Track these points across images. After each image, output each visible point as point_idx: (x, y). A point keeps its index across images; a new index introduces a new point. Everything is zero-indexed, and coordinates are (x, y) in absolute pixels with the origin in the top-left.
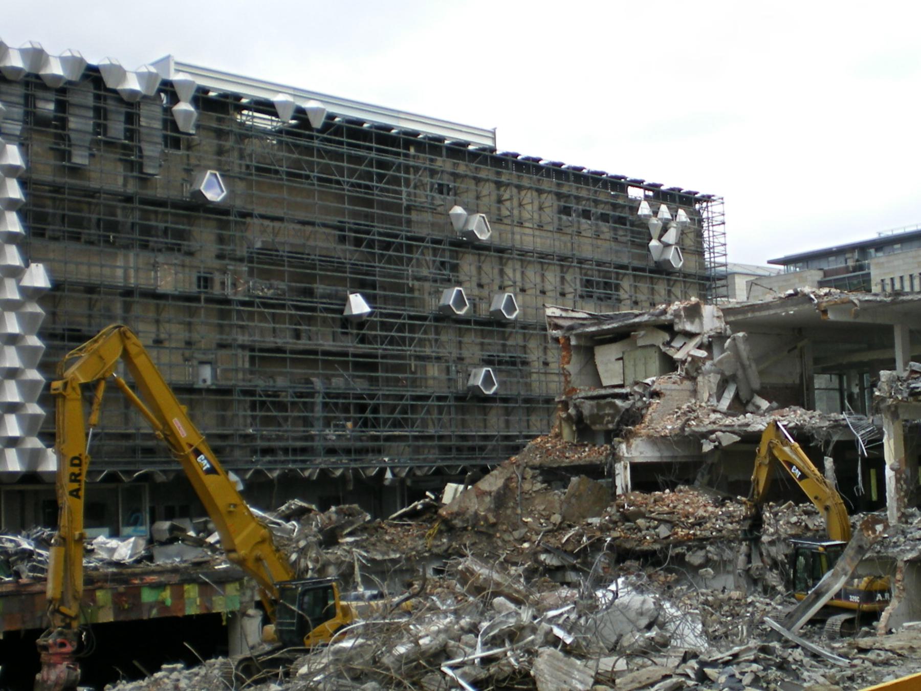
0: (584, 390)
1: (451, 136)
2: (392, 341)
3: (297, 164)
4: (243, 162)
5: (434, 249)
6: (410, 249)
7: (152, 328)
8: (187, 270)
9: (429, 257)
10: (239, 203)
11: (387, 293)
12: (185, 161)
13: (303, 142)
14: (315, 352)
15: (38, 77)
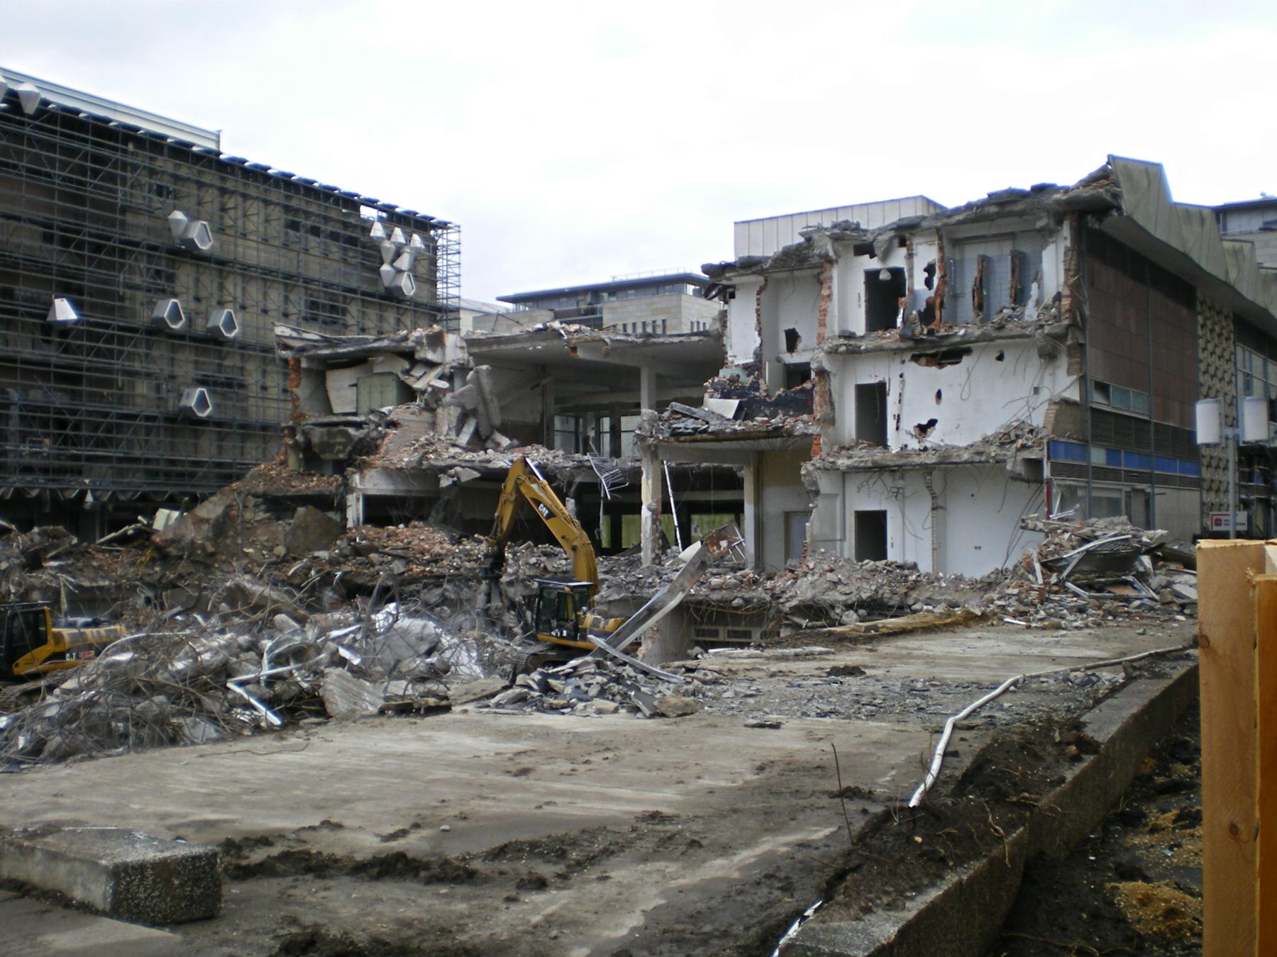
0: (314, 416)
2: (99, 353)
5: (149, 256)
6: (123, 253)
11: (94, 300)
13: (13, 128)
14: (14, 360)
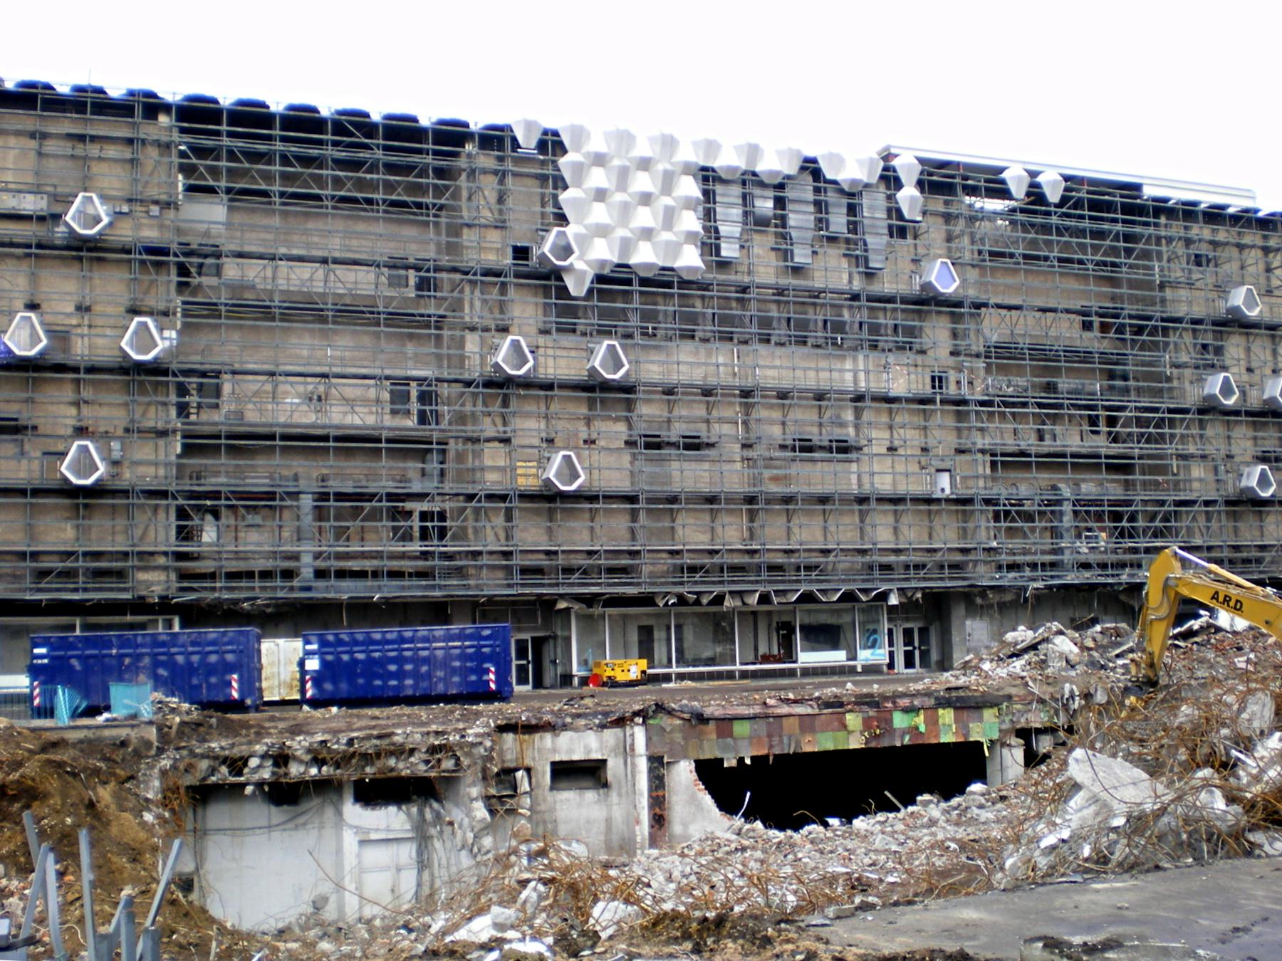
1: (1206, 200)
3: (1033, 244)
4: (976, 248)
6: (1165, 331)
7: (887, 435)
8: (920, 369)
9: (1188, 338)
10: (972, 293)
11: (1141, 384)
12: (912, 250)
13: (1039, 220)
15: (754, 174)
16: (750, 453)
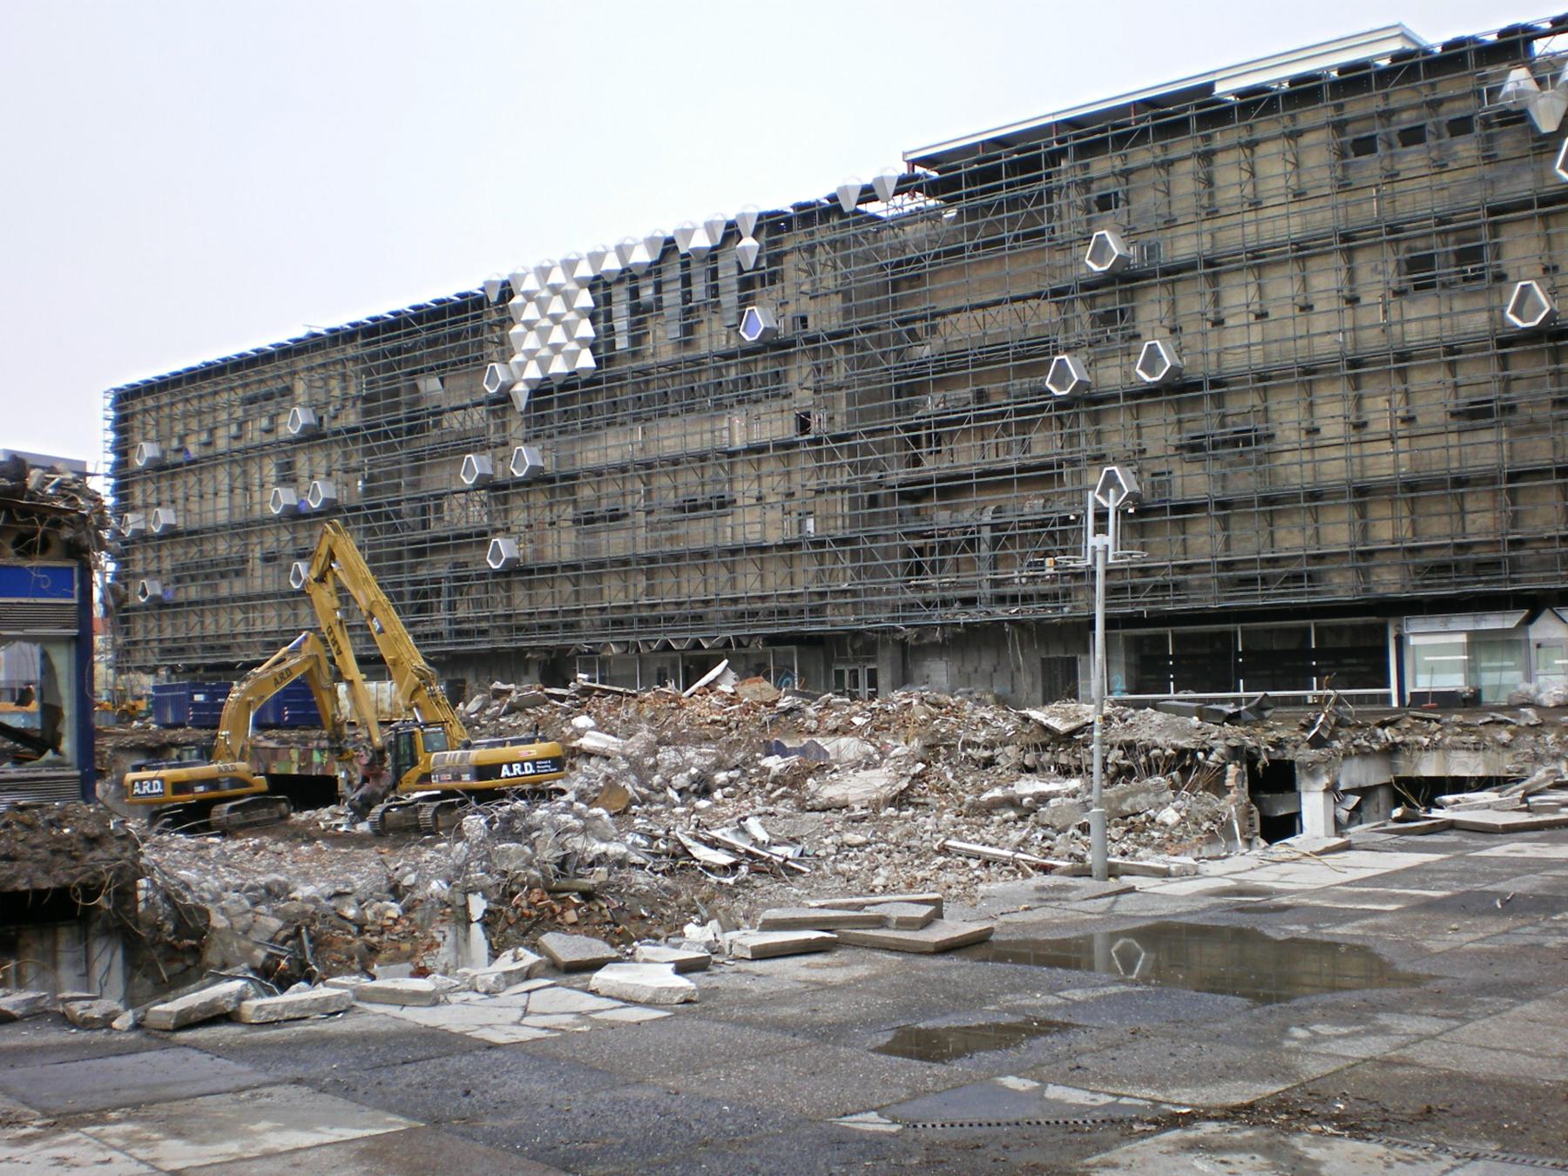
16: (654, 518)
